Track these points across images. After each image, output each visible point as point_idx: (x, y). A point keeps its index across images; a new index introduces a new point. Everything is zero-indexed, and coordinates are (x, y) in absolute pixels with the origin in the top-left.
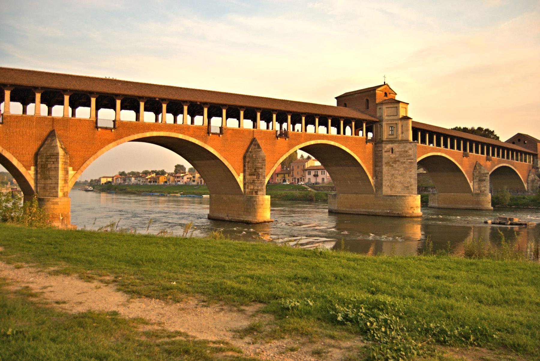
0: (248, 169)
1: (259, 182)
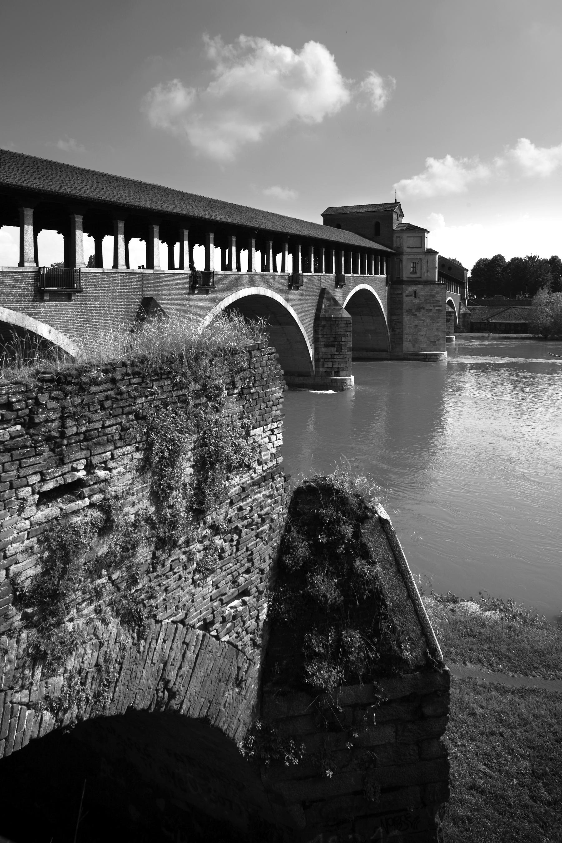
0: (323, 337)
1: (342, 356)
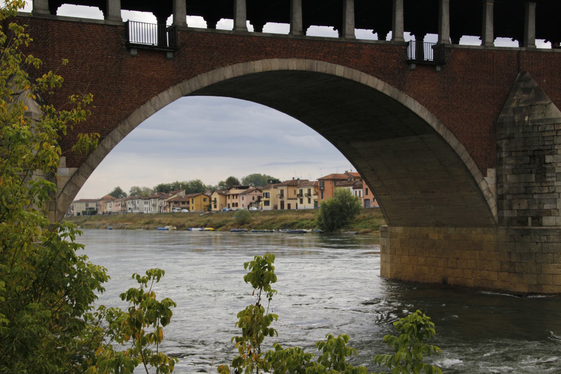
0: (510, 156)
